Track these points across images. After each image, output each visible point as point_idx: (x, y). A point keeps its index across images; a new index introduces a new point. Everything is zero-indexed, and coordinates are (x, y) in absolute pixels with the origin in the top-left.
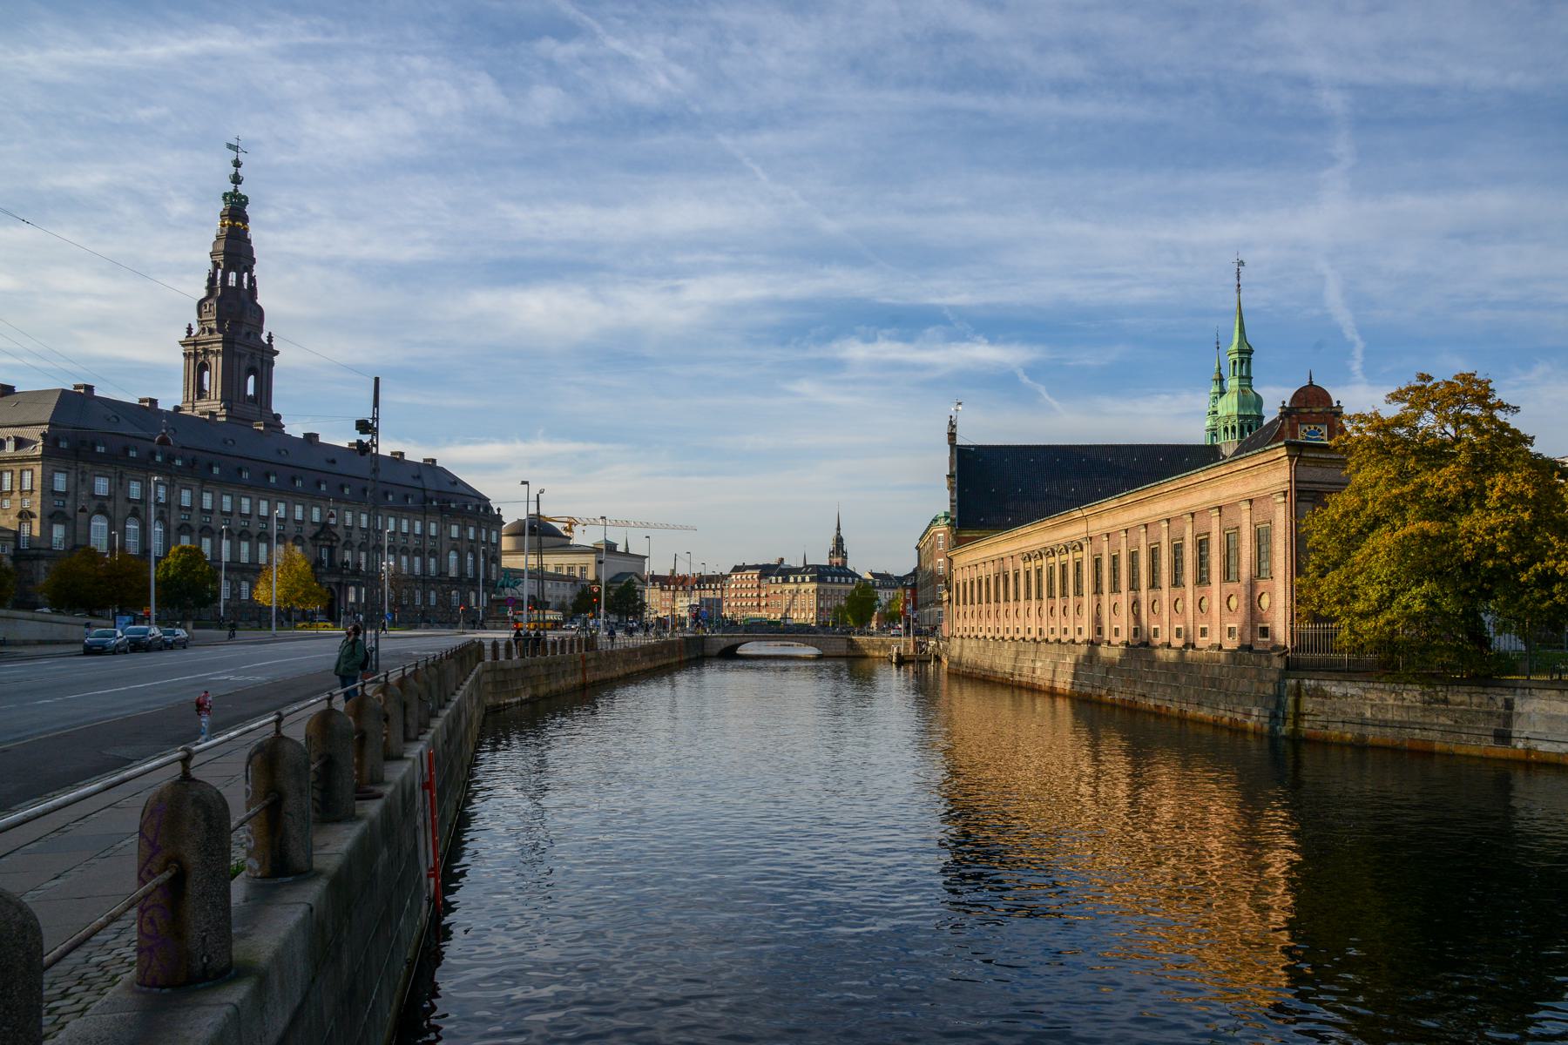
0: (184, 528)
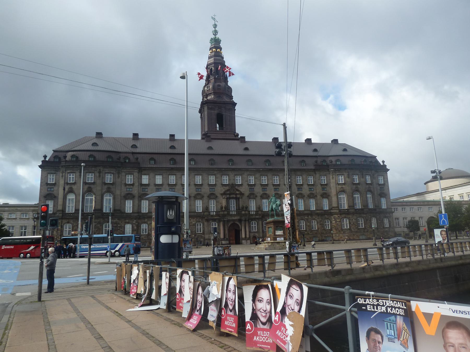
0: (129, 196)
